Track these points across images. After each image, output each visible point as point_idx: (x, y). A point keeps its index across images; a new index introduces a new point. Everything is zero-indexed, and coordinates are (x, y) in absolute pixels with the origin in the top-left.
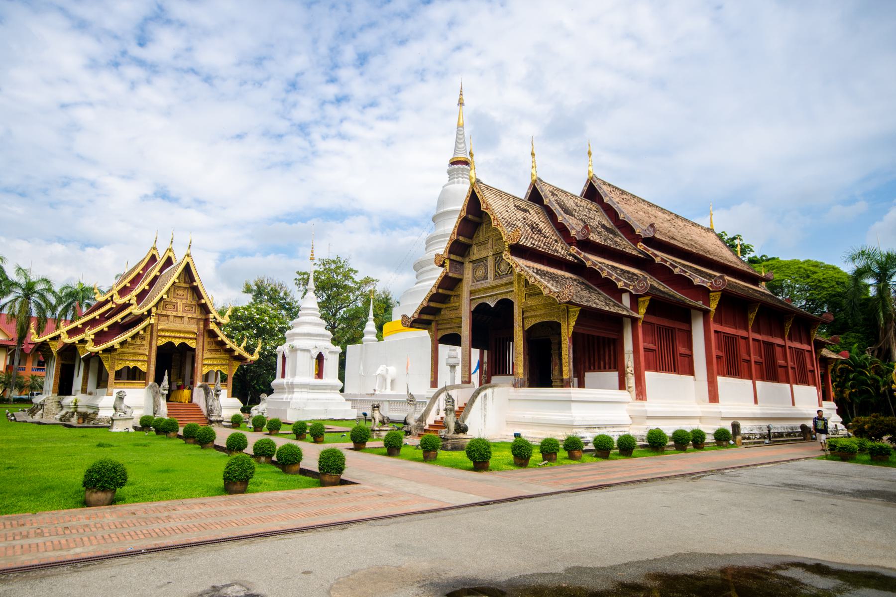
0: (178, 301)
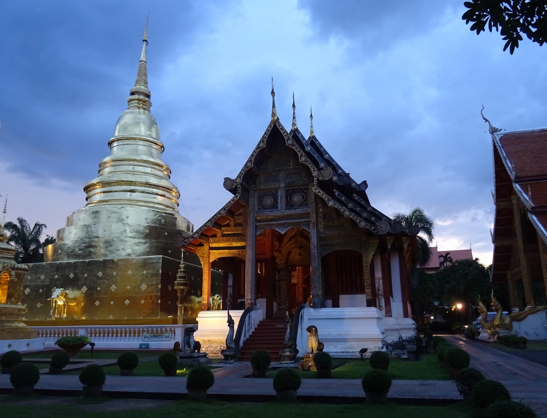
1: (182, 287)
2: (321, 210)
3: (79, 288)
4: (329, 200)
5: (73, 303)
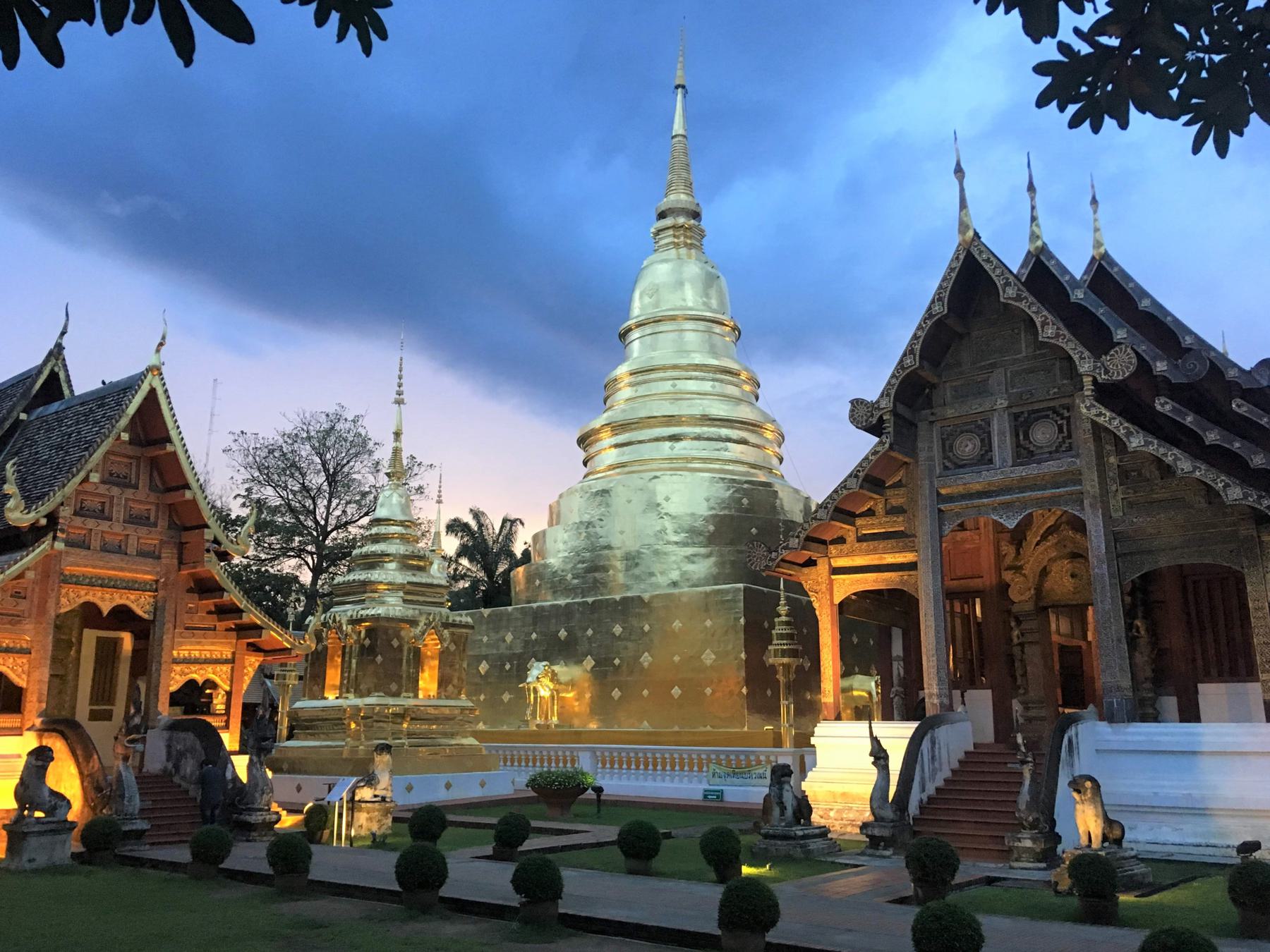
0: (115, 491)
1: (785, 660)
2: (1112, 460)
3: (579, 662)
4: (1129, 434)
5: (567, 691)
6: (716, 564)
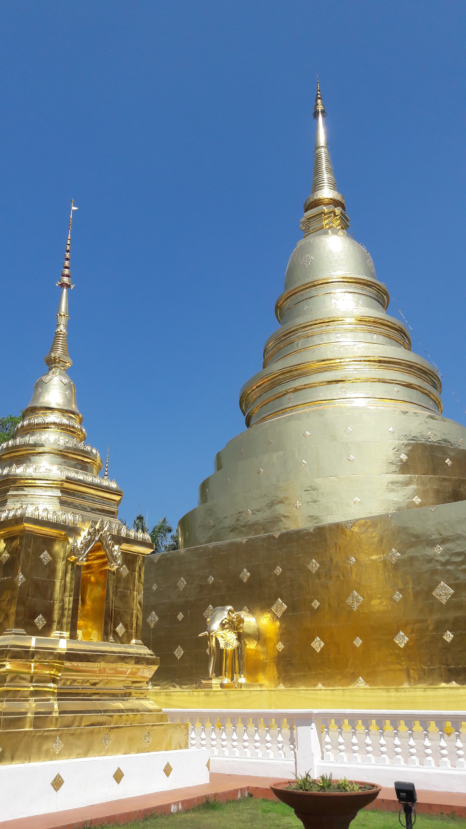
6: (416, 493)
